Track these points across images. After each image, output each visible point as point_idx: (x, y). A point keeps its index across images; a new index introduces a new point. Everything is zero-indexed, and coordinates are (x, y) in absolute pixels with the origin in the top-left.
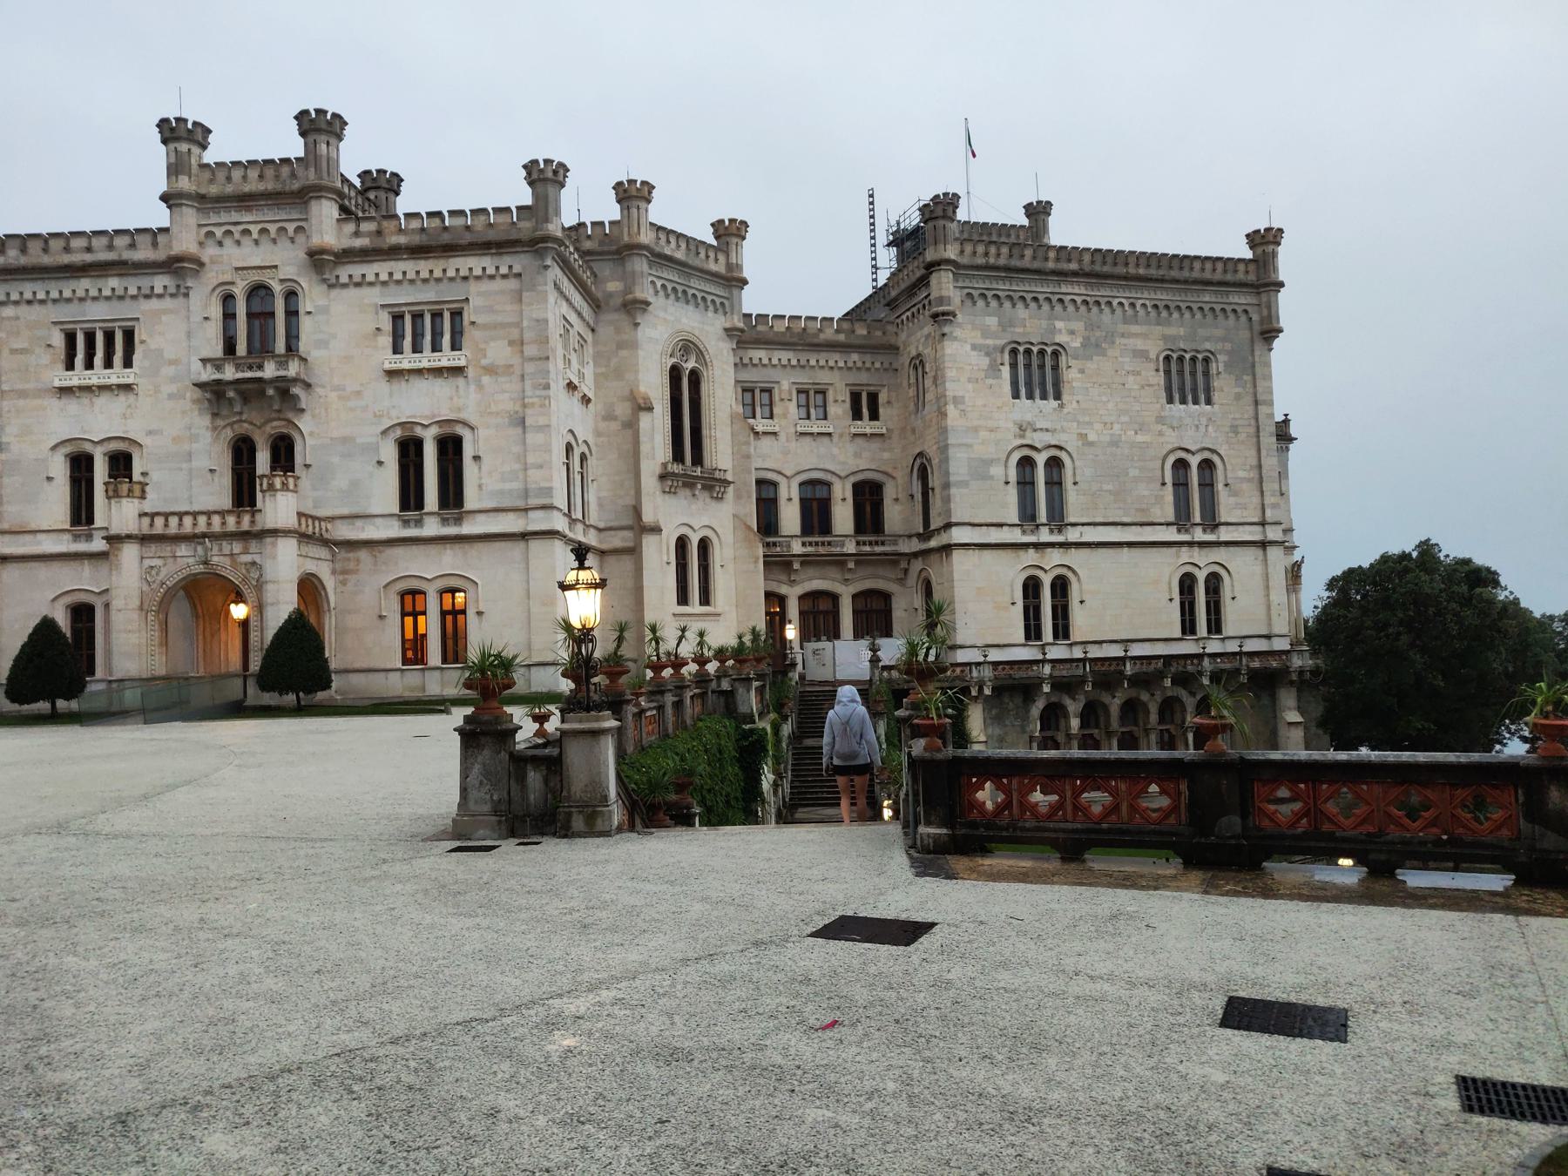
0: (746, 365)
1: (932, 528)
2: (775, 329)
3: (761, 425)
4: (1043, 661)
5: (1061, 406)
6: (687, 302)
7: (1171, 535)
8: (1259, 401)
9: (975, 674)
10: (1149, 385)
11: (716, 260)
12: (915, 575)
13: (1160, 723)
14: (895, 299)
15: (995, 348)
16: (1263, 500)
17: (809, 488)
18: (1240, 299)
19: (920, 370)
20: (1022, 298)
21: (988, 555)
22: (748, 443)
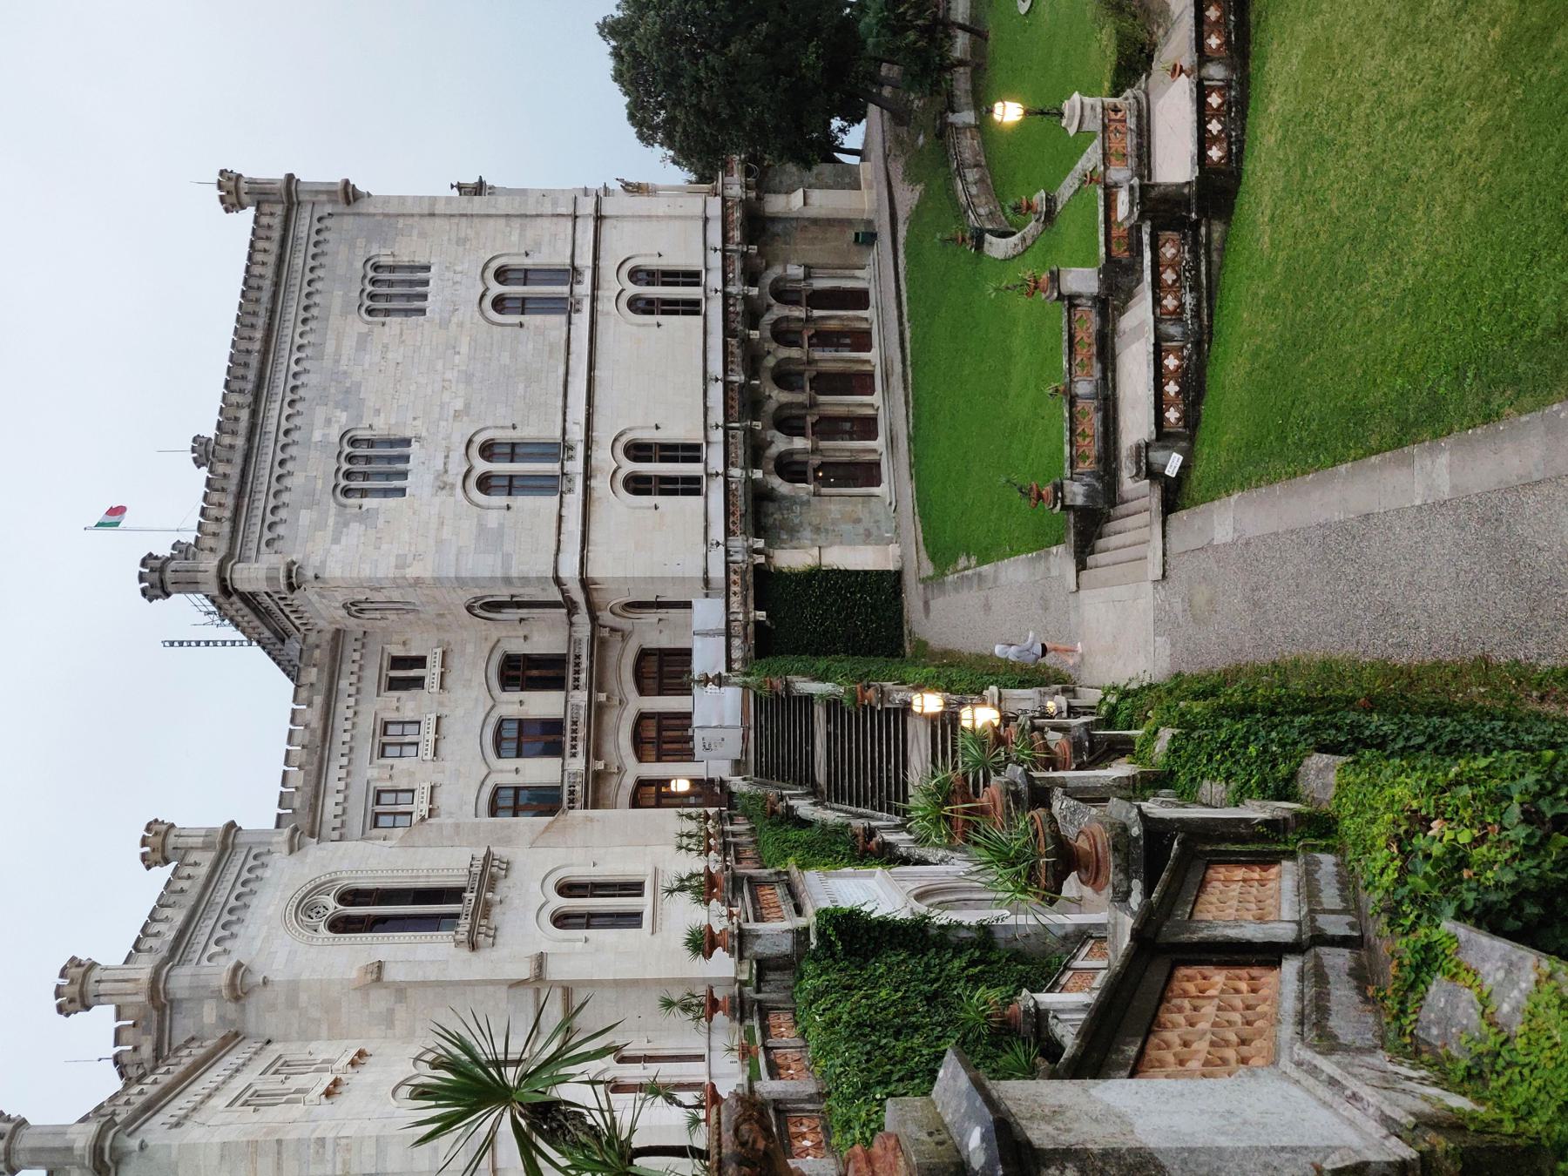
0: (343, 823)
1: (560, 598)
2: (300, 783)
3: (421, 806)
4: (726, 476)
5: (418, 439)
6: (246, 906)
7: (582, 321)
8: (431, 212)
9: (738, 558)
10: (401, 334)
11: (196, 864)
12: (618, 619)
13: (801, 347)
14: (275, 632)
15: (338, 515)
16: (547, 216)
17: (505, 745)
18: (304, 225)
19: (364, 606)
20: (279, 478)
21: (594, 535)
22: (440, 826)
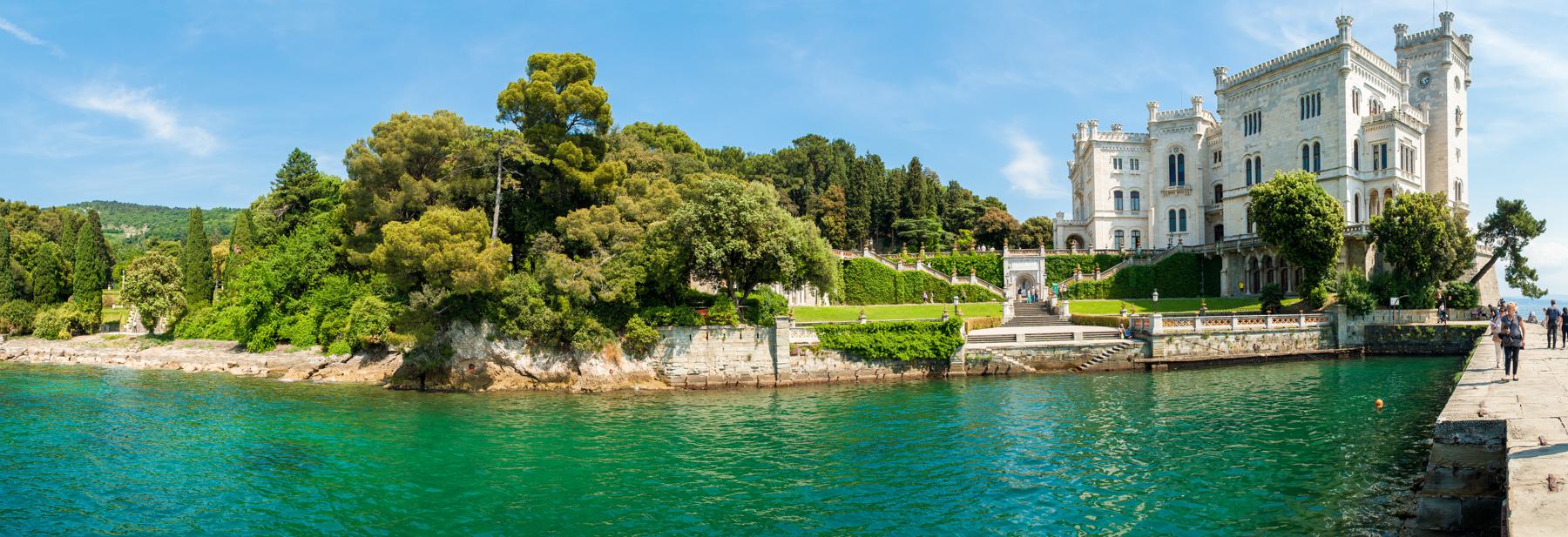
21: (1234, 200)
